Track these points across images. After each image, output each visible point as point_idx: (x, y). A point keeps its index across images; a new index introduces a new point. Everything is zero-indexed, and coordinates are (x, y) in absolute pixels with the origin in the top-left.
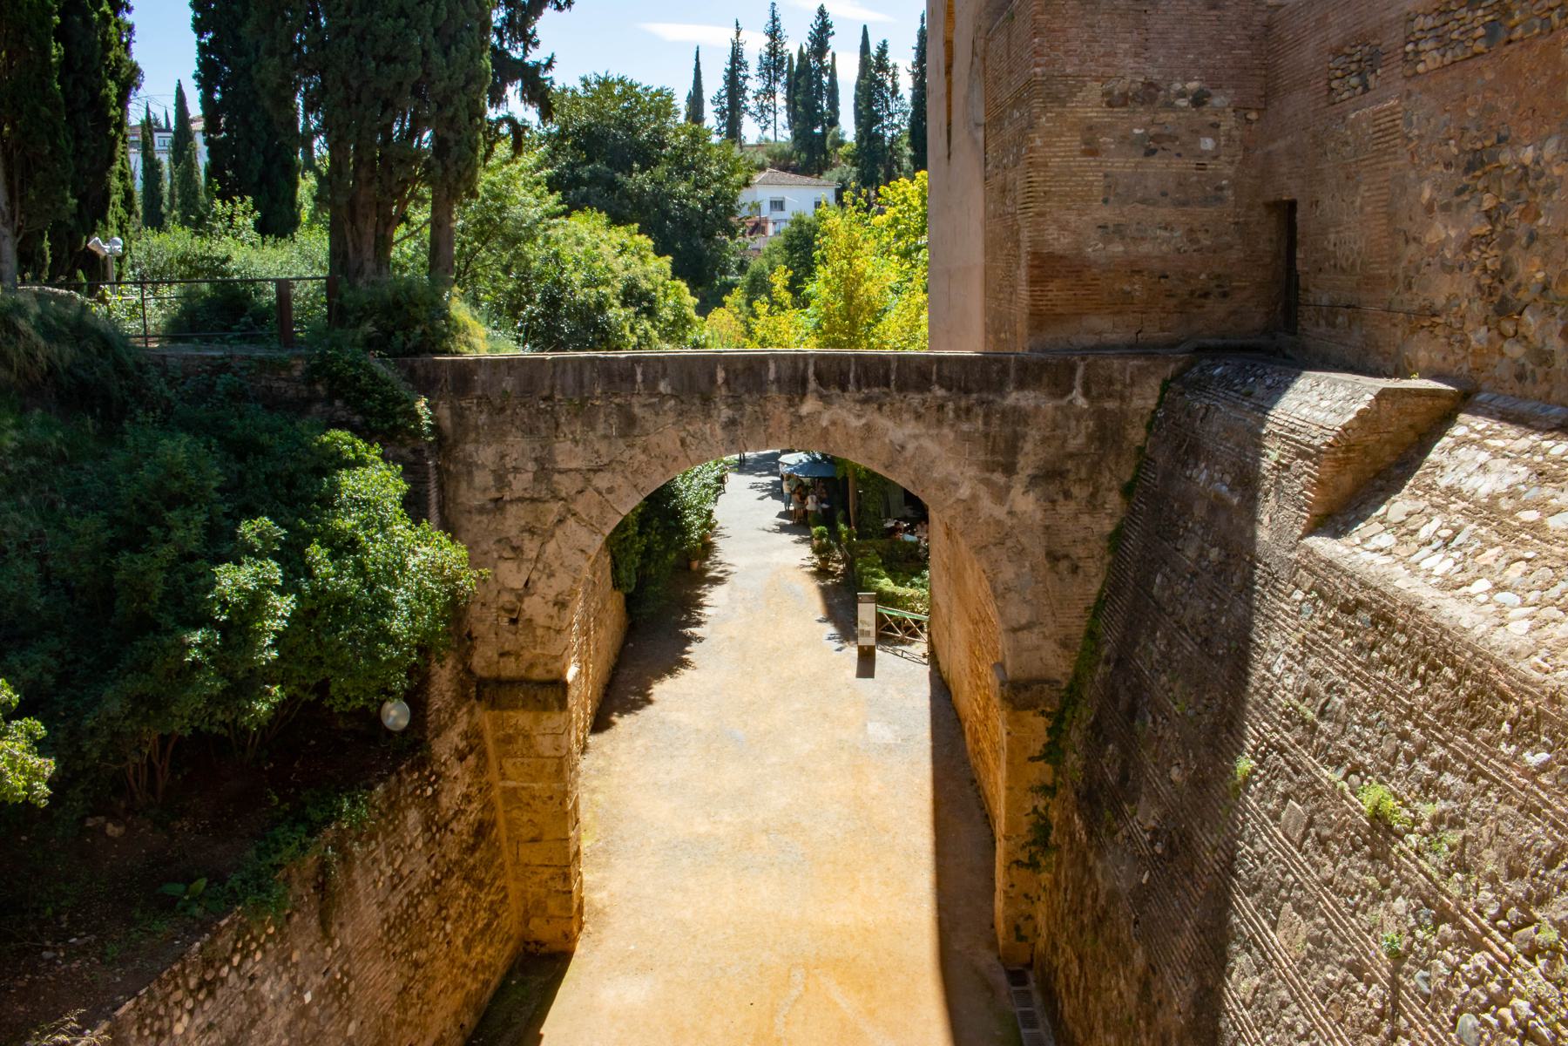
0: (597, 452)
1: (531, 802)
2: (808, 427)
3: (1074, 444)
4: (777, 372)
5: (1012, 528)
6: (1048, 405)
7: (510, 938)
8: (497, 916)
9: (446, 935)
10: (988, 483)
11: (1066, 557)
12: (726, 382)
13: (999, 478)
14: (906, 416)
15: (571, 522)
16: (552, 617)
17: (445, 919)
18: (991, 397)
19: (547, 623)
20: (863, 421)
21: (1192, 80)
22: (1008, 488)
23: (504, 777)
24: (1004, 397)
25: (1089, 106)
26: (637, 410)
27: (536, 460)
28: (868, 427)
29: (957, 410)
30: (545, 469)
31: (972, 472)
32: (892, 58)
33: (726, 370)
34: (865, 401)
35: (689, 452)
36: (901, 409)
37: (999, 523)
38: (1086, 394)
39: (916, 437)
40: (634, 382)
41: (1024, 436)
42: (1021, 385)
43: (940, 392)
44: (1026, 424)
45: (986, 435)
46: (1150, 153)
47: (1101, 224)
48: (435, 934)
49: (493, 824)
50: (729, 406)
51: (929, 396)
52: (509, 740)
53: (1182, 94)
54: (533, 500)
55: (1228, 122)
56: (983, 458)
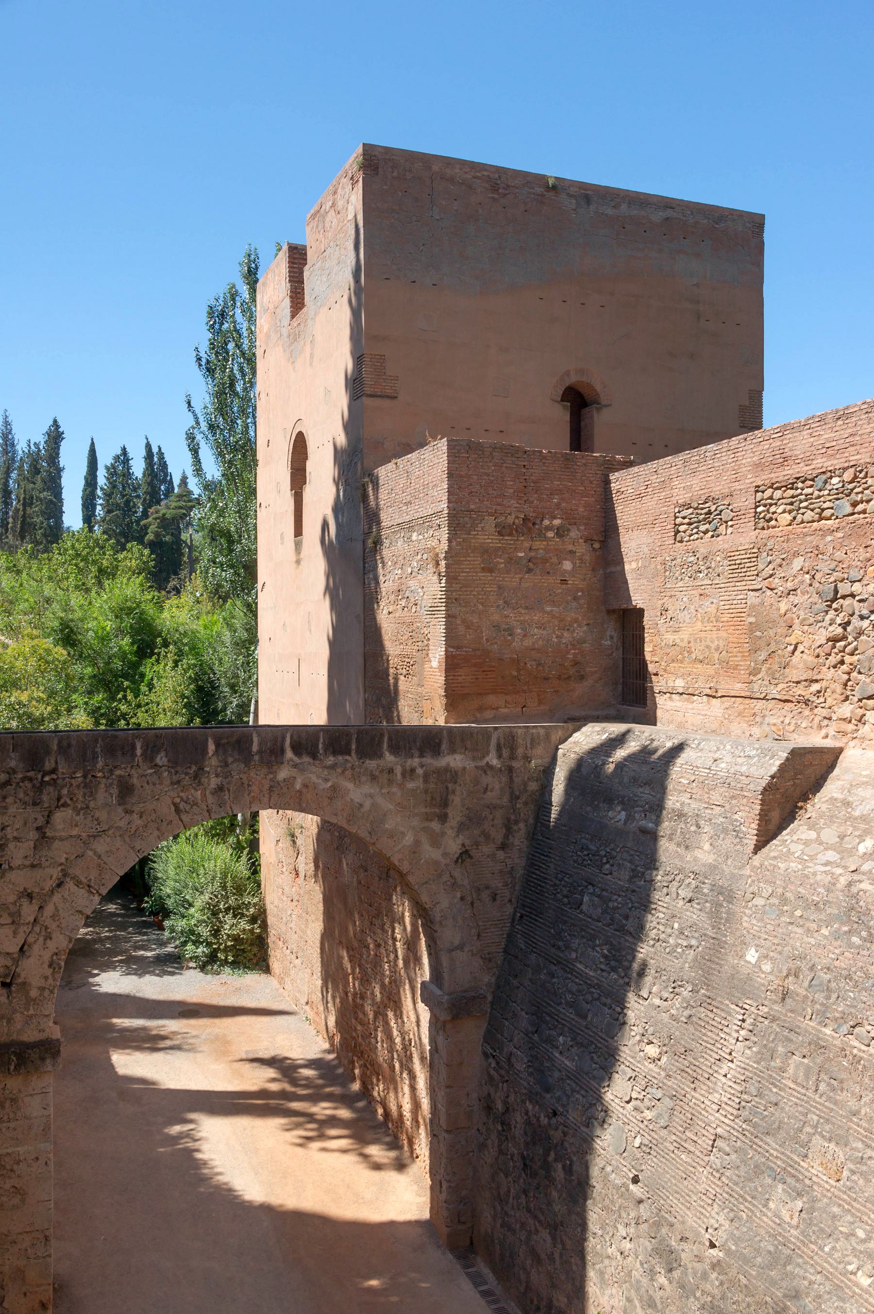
1: (15, 1167)
2: (285, 790)
3: (491, 797)
4: (260, 744)
5: (447, 865)
6: (470, 765)
11: (487, 888)
12: (216, 752)
13: (435, 825)
14: (364, 779)
15: (70, 885)
16: (46, 978)
19: (42, 983)
20: (329, 784)
21: (555, 518)
22: (443, 834)
26: (135, 781)
27: (37, 829)
28: (334, 788)
29: (403, 774)
30: (43, 838)
31: (415, 822)
34: (333, 767)
36: (360, 773)
37: (436, 863)
38: (500, 756)
39: (371, 796)
40: (134, 755)
41: (454, 792)
42: (453, 751)
43: (389, 758)
44: (455, 783)
45: (426, 791)
46: (529, 571)
47: (495, 624)
50: (217, 776)
51: (381, 763)
53: (548, 528)
56: (424, 810)
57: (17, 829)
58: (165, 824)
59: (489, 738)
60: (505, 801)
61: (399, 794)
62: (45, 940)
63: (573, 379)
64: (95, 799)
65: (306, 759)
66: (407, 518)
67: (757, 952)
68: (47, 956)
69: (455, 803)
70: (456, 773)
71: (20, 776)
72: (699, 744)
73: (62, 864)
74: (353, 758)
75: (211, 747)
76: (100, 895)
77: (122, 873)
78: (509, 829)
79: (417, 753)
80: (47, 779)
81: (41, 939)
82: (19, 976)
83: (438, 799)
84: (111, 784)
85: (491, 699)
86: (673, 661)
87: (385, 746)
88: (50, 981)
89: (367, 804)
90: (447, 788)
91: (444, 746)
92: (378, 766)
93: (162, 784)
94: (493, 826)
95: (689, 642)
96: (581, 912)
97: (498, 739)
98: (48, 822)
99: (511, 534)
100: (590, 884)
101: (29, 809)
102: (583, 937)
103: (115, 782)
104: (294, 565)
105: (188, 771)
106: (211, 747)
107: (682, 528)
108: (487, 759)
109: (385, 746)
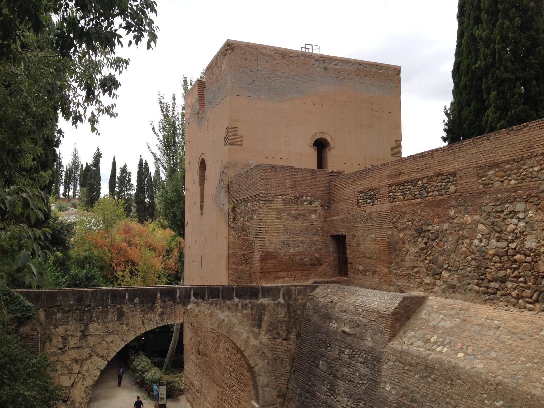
0: (108, 327)
2: (191, 314)
4: (180, 293)
5: (261, 347)
6: (271, 303)
10: (252, 331)
12: (161, 298)
13: (256, 330)
14: (225, 309)
16: (83, 398)
18: (253, 301)
19: (81, 400)
20: (210, 311)
22: (260, 333)
25: (278, 204)
26: (125, 310)
27: (81, 331)
28: (212, 313)
29: (242, 306)
30: (84, 336)
32: (129, 169)
33: (161, 293)
34: (211, 303)
35: (145, 326)
37: (256, 347)
38: (284, 299)
41: (264, 314)
42: (264, 296)
43: (236, 300)
45: (252, 314)
46: (297, 219)
53: (305, 201)
54: (78, 348)
55: (320, 210)
56: (251, 323)
57: (72, 331)
58: (137, 329)
59: (279, 291)
60: (286, 319)
62: (83, 381)
63: (319, 136)
64: (107, 318)
65: (200, 300)
66: (246, 196)
67: (390, 386)
68: (83, 388)
69: (265, 319)
70: (265, 306)
71: (74, 308)
72: (367, 294)
73: (91, 347)
74: (220, 300)
76: (108, 361)
77: (117, 351)
78: (289, 332)
79: (248, 298)
80: (86, 309)
81: (81, 380)
82: (71, 397)
83: (257, 318)
84: (114, 312)
85: (282, 274)
86: (358, 258)
87: (234, 294)
88: (85, 400)
89: (226, 320)
90: (261, 313)
91: (260, 296)
92: (231, 303)
93: (136, 311)
94: (281, 330)
95: (364, 250)
96: (319, 369)
97: (284, 291)
98: (86, 328)
99: (289, 204)
100: (322, 356)
101: (78, 323)
102: (319, 380)
103: (116, 310)
104: (200, 215)
105: (148, 305)
107: (360, 201)
108: (279, 300)
109: (234, 294)
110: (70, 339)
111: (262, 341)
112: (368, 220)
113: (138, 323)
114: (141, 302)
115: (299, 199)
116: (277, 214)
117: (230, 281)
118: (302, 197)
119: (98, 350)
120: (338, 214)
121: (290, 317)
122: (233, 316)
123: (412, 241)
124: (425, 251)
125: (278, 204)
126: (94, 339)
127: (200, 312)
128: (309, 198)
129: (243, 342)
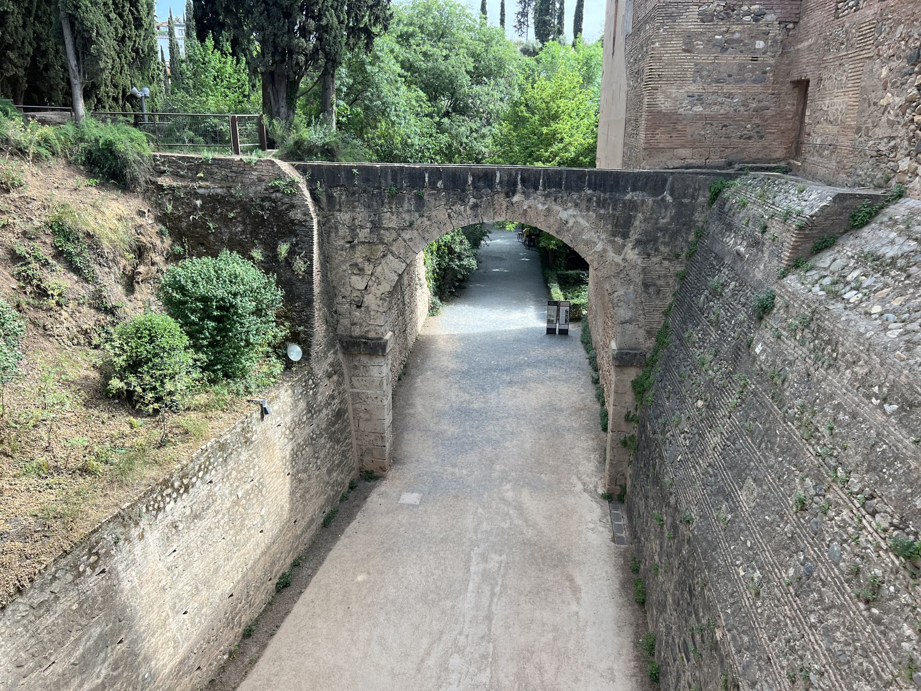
6: (650, 200)
7: (353, 469)
8: (346, 458)
9: (317, 466)
10: (613, 242)
11: (655, 285)
12: (473, 182)
13: (619, 240)
14: (569, 205)
16: (379, 306)
17: (317, 458)
20: (546, 206)
23: (352, 387)
24: (625, 195)
25: (690, 21)
28: (549, 210)
30: (376, 226)
33: (473, 176)
34: (547, 196)
37: (617, 264)
39: (574, 216)
47: (690, 94)
48: (311, 466)
49: (346, 411)
52: (356, 367)
53: (748, 13)
54: (369, 242)
55: (775, 31)
58: (442, 225)
59: (666, 180)
61: (594, 215)
65: (532, 190)
68: (378, 295)
69: (635, 225)
75: (470, 179)
88: (381, 308)
99: (712, 20)
106: (470, 179)
110: (358, 230)
111: (627, 257)
112: (843, 44)
113: (443, 217)
114: (446, 188)
115: (733, 10)
116: (686, 44)
117: (625, 163)
118: (741, 6)
119: (393, 249)
120: (807, 36)
121: (678, 224)
122: (583, 217)
123: (898, 84)
124: (914, 104)
125: (690, 21)
126: (387, 233)
127: (530, 207)
128: (757, 6)
129: (596, 256)
